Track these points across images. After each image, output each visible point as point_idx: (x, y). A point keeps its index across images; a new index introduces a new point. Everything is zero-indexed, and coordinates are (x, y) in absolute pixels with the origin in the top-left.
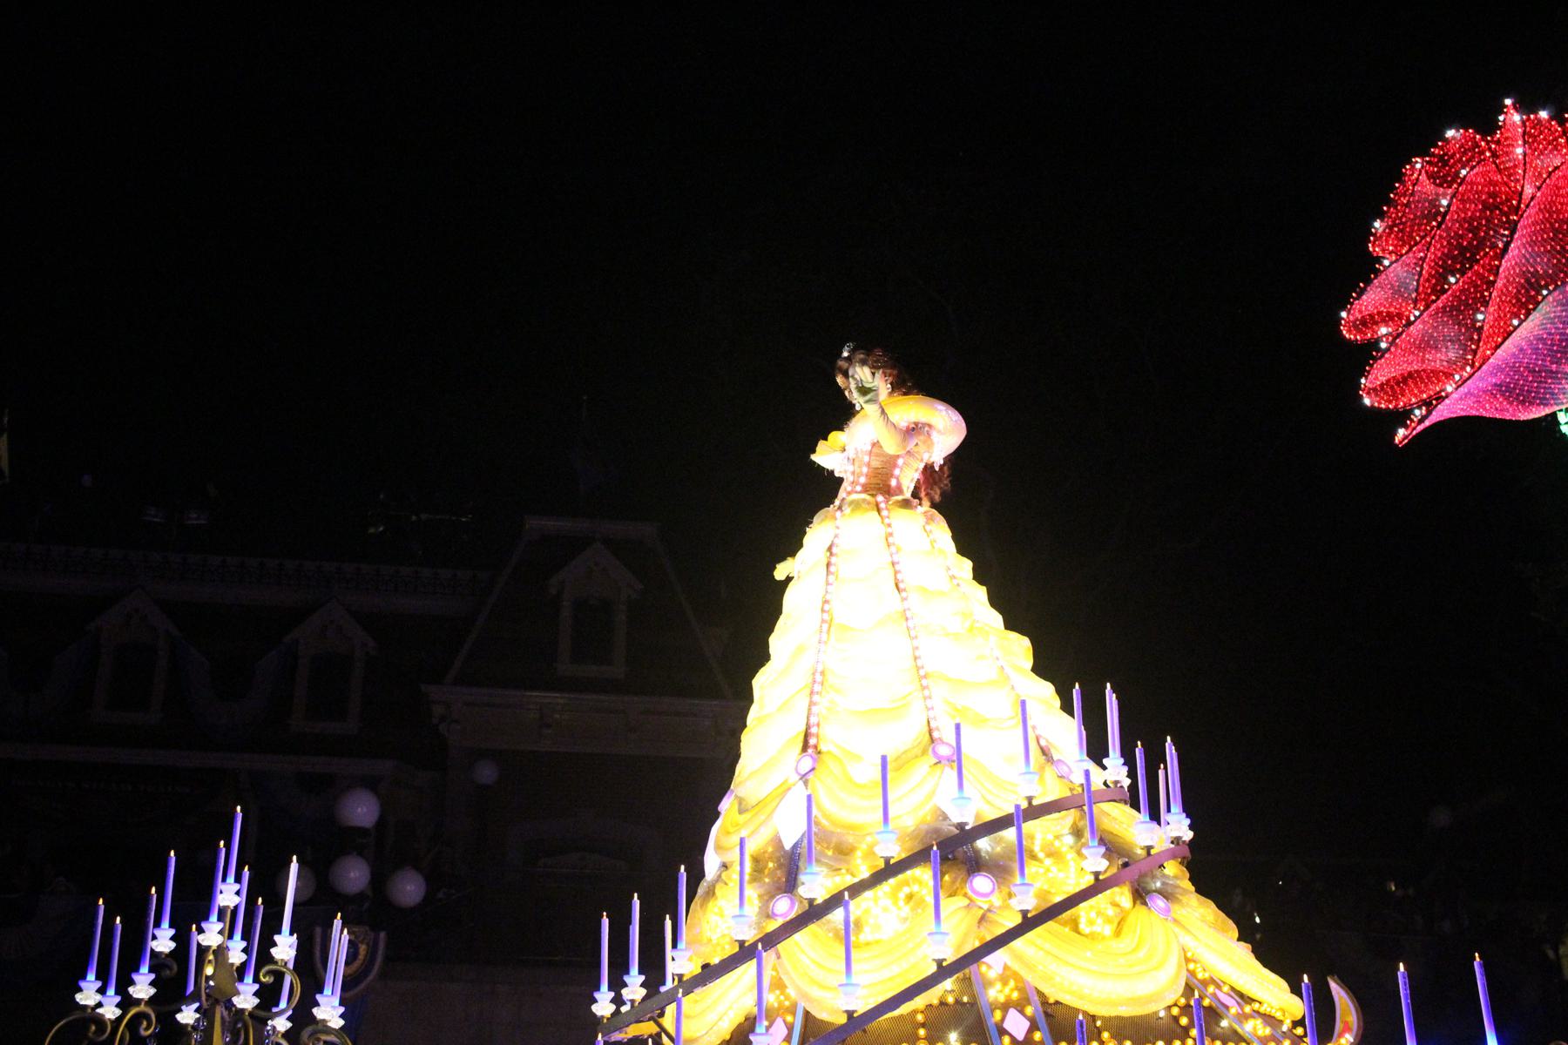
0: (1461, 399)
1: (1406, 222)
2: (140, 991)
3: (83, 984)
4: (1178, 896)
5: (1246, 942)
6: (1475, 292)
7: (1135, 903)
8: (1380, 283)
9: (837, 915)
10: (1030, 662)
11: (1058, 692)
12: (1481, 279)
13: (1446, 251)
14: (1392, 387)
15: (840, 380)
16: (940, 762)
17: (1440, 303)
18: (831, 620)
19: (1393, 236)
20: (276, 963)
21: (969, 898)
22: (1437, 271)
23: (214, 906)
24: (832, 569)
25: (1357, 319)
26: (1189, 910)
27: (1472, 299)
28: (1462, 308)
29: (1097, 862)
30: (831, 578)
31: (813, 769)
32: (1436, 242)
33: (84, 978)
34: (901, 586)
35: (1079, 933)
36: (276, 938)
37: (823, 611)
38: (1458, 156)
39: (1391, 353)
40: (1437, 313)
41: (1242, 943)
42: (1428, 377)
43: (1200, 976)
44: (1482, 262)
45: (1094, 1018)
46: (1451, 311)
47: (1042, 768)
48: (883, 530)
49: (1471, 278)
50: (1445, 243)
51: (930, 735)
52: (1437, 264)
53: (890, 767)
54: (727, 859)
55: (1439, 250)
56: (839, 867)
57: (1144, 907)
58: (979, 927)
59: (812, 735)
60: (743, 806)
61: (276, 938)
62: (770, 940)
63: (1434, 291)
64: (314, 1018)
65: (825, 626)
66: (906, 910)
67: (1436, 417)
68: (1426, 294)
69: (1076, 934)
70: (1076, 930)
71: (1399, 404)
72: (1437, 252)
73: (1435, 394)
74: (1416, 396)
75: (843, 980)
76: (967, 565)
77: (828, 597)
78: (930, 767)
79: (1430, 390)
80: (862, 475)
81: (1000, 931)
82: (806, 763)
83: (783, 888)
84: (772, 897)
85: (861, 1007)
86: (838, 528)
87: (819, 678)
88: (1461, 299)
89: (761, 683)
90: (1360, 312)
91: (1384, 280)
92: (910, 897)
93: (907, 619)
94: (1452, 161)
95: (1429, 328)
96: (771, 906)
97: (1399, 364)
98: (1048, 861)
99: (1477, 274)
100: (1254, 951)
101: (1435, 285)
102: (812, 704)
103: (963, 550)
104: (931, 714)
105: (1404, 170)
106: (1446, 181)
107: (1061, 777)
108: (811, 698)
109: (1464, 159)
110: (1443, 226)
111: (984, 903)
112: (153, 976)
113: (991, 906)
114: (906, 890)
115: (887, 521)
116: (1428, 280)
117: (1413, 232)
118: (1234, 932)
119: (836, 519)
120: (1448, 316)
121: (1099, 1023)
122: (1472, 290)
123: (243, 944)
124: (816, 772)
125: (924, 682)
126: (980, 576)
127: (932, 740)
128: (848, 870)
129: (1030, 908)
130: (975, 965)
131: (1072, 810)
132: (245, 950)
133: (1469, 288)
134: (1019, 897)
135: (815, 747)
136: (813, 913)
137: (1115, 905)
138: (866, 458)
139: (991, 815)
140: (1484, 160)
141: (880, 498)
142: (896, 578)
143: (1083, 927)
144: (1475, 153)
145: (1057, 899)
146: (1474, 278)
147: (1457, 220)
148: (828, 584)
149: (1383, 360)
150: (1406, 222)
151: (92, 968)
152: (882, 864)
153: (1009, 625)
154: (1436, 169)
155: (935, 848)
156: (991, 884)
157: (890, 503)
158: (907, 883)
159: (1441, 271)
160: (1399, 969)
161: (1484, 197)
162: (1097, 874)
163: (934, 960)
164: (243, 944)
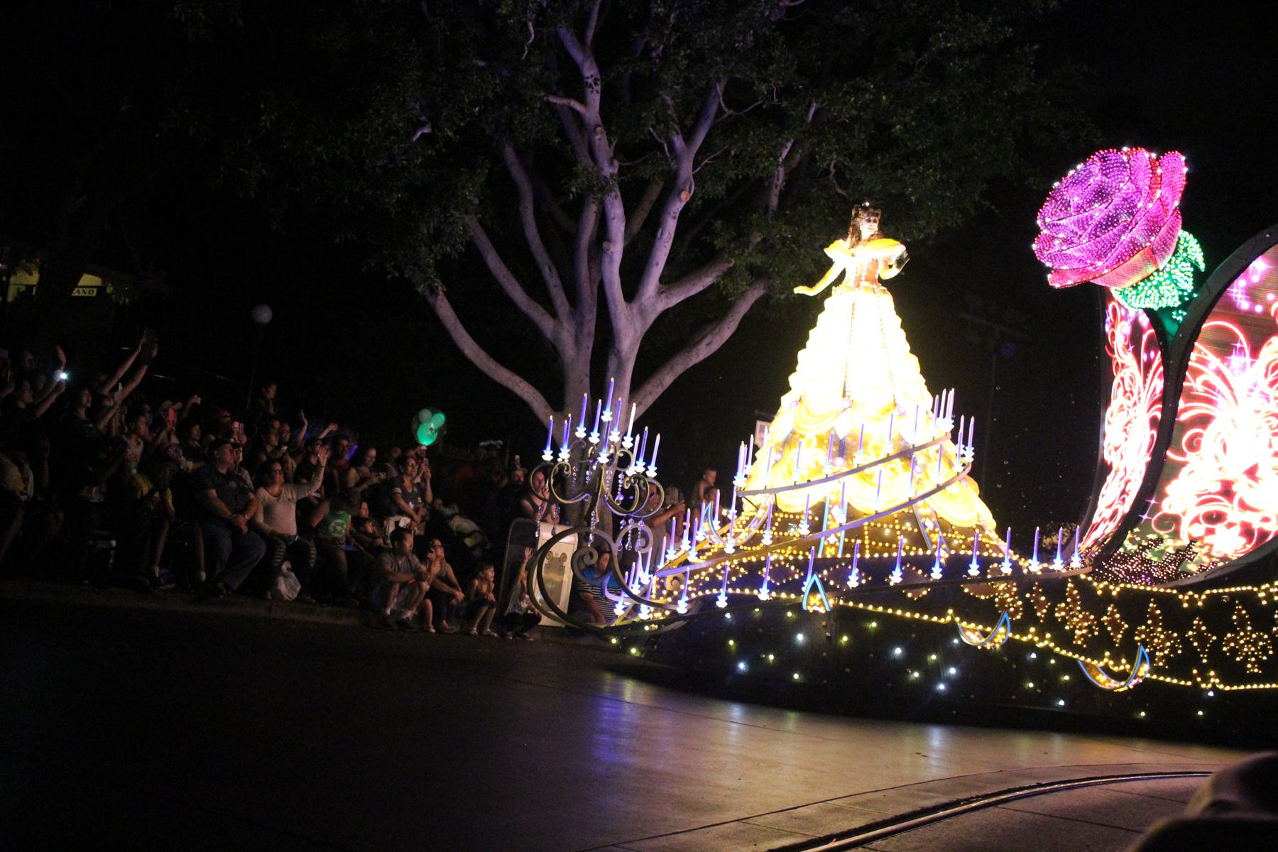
45: (951, 526)
81: (928, 490)
85: (880, 510)
121: (954, 527)
136: (859, 469)
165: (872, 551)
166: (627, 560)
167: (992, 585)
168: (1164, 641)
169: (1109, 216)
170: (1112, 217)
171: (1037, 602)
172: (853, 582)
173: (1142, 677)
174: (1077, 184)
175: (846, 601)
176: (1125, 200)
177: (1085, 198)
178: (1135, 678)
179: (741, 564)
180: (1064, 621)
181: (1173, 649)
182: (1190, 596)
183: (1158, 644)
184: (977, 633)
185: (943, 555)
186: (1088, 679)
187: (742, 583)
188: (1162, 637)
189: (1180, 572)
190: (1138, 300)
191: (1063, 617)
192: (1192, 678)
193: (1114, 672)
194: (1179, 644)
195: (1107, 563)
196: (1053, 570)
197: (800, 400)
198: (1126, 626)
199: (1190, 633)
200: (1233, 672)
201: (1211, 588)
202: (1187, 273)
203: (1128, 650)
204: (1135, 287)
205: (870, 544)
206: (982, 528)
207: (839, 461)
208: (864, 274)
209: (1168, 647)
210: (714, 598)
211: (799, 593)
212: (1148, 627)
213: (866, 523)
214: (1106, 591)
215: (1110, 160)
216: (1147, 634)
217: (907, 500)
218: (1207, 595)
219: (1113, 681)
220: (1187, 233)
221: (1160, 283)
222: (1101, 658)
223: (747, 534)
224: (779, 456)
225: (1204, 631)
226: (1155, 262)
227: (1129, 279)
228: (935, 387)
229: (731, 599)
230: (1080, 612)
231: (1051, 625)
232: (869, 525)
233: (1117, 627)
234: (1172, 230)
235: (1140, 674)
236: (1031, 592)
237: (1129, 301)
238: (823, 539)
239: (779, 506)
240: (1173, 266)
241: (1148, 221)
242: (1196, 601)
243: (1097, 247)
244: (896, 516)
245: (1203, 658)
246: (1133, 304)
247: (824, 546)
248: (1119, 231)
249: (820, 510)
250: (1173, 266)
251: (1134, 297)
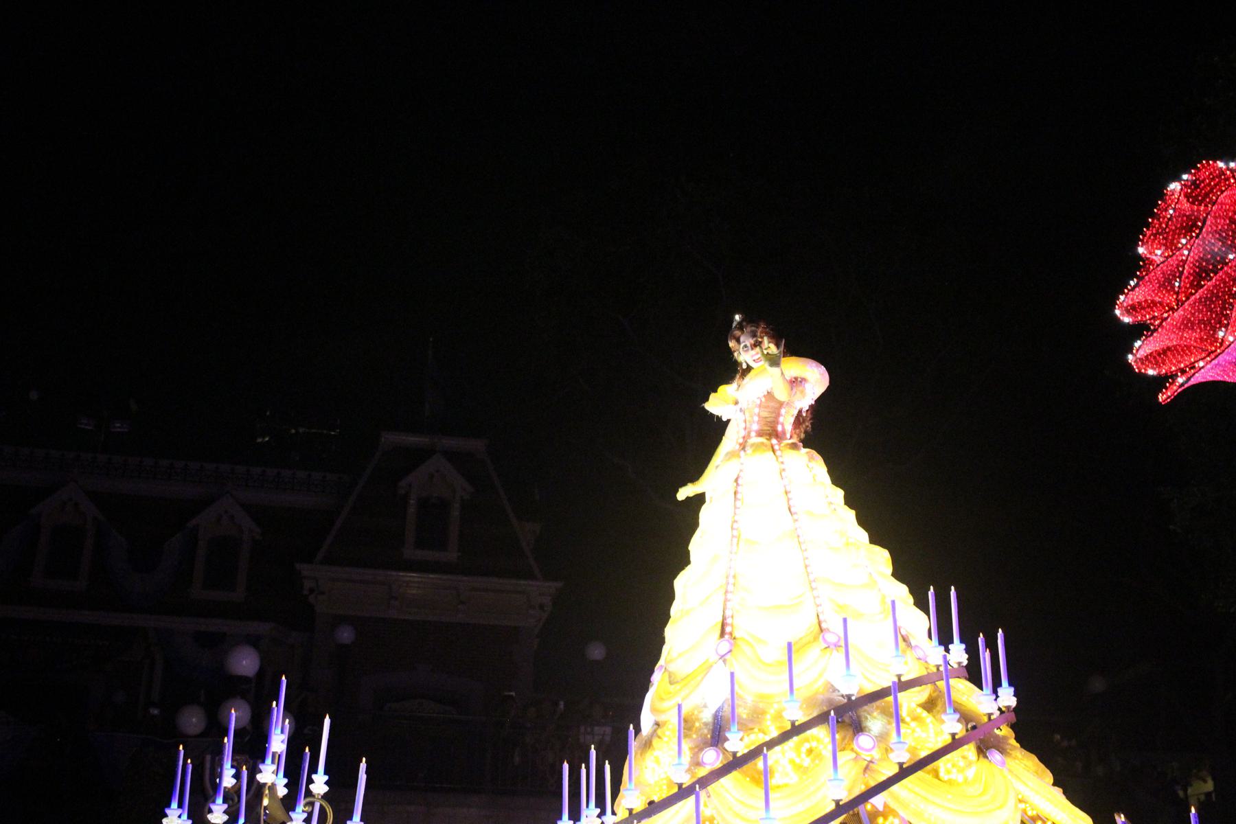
0: (1212, 368)
1: (1169, 232)
2: (216, 818)
3: (168, 811)
4: (1008, 751)
5: (1059, 787)
6: (1225, 287)
7: (979, 757)
8: (1149, 278)
9: (759, 762)
10: (890, 569)
11: (912, 592)
12: (1228, 277)
13: (1202, 256)
14: (1155, 358)
15: (732, 344)
16: (829, 647)
17: (1197, 296)
18: (740, 535)
19: (1156, 242)
20: (314, 796)
21: (856, 753)
22: (1195, 271)
23: (269, 753)
24: (739, 496)
25: (1129, 305)
26: (1017, 761)
27: (1222, 292)
28: (1214, 299)
29: (953, 726)
31: (730, 651)
32: (1195, 248)
33: (169, 806)
34: (792, 510)
35: (939, 779)
37: (732, 529)
38: (1207, 181)
39: (1158, 333)
40: (1195, 303)
41: (1056, 788)
42: (1183, 350)
43: (1031, 813)
44: (1230, 264)
46: (1205, 302)
47: (904, 651)
49: (1221, 277)
50: (1201, 249)
51: (820, 626)
52: (1194, 265)
53: (794, 648)
54: (661, 719)
55: (1197, 254)
56: (752, 727)
57: (986, 760)
58: (864, 775)
59: (727, 624)
60: (672, 679)
62: (704, 782)
63: (1192, 286)
65: (735, 540)
66: (807, 761)
67: (1193, 381)
68: (1186, 287)
69: (937, 781)
70: (937, 776)
71: (1162, 371)
72: (1195, 256)
73: (1191, 364)
74: (1174, 365)
75: (763, 813)
76: (839, 493)
77: (737, 518)
78: (821, 650)
79: (1185, 361)
80: (754, 422)
81: (882, 778)
82: (724, 646)
83: (710, 742)
84: (701, 749)
86: (742, 464)
87: (731, 580)
88: (1213, 293)
89: (682, 583)
90: (1132, 299)
91: (1153, 276)
92: (810, 751)
94: (1203, 185)
95: (1188, 314)
96: (701, 756)
97: (1162, 341)
98: (913, 724)
99: (1227, 274)
100: (1065, 793)
101: (1193, 281)
102: (726, 600)
103: (836, 481)
104: (820, 609)
105: (1165, 191)
106: (1197, 200)
107: (919, 659)
108: (726, 596)
109: (1212, 183)
110: (1200, 237)
111: (867, 756)
112: (225, 806)
113: (873, 758)
114: (807, 746)
115: (780, 459)
116: (1188, 277)
117: (1174, 240)
118: (1049, 778)
119: (740, 457)
120: (1203, 305)
122: (1222, 285)
123: (233, 771)
124: (733, 653)
125: (814, 585)
126: (849, 502)
127: (821, 630)
128: (759, 730)
129: (905, 761)
130: (862, 805)
131: (929, 685)
132: (235, 776)
133: (1220, 284)
134: (896, 752)
135: (731, 634)
136: (735, 763)
137: (964, 757)
138: (757, 410)
139: (870, 688)
140: (1229, 185)
141: (774, 441)
142: (788, 504)
143: (942, 774)
144: (1222, 179)
145: (923, 754)
146: (1224, 277)
147: (1210, 232)
148: (736, 508)
149: (1152, 338)
150: (1169, 232)
151: (175, 797)
152: (789, 727)
153: (874, 540)
154: (1189, 191)
155: (832, 713)
156: (872, 742)
157: (782, 445)
158: (807, 740)
159: (1197, 270)
160: (1190, 811)
161: (1230, 214)
162: (953, 735)
163: (833, 800)
164: (233, 771)
208: (755, 427)
217: (832, 806)
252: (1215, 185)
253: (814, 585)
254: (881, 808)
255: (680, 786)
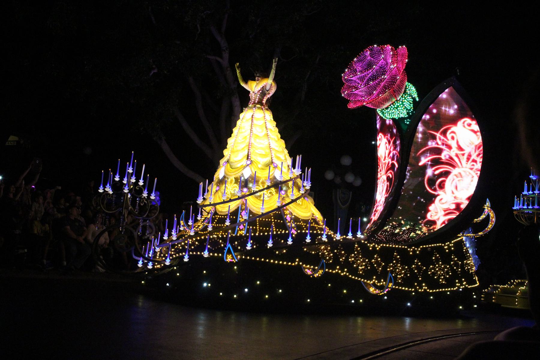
10: (285, 146)
24: (253, 121)
30: (253, 123)
31: (250, 164)
36: (140, 180)
45: (299, 219)
48: (263, 115)
61: (140, 180)
64: (150, 198)
66: (270, 195)
75: (262, 207)
81: (287, 202)
82: (249, 162)
85: (265, 211)
93: (268, 136)
99: (376, 82)
121: (300, 220)
125: (271, 150)
158: (270, 190)
165: (260, 232)
166: (144, 241)
167: (318, 246)
168: (401, 270)
169: (374, 75)
170: (375, 76)
171: (340, 254)
172: (249, 247)
173: (390, 288)
174: (360, 61)
175: (246, 256)
176: (381, 68)
177: (363, 67)
178: (387, 288)
179: (197, 240)
180: (353, 262)
181: (405, 274)
182: (413, 249)
183: (399, 272)
184: (310, 270)
185: (294, 232)
186: (365, 289)
187: (196, 250)
188: (400, 268)
189: (410, 238)
190: (388, 114)
191: (352, 261)
192: (415, 287)
193: (378, 285)
194: (408, 271)
195: (377, 235)
196: (348, 239)
197: (228, 161)
198: (383, 264)
199: (413, 266)
200: (433, 283)
201: (423, 245)
202: (410, 102)
203: (383, 275)
204: (387, 108)
205: (259, 229)
206: (315, 221)
207: (245, 190)
209: (403, 273)
210: (183, 257)
211: (223, 254)
212: (394, 264)
213: (258, 219)
214: (374, 247)
215: (374, 50)
216: (393, 268)
218: (421, 248)
219: (377, 290)
220: (409, 84)
221: (398, 107)
222: (371, 280)
223: (202, 226)
224: (218, 188)
225: (420, 265)
226: (396, 97)
227: (384, 104)
228: (292, 154)
229: (190, 257)
230: (361, 258)
231: (347, 265)
232: (259, 220)
233: (379, 265)
234: (402, 82)
235: (389, 286)
236: (337, 249)
237: (385, 115)
238: (237, 226)
239: (217, 212)
240: (403, 99)
241: (391, 77)
242: (416, 251)
243: (368, 89)
244: (272, 215)
245: (420, 277)
246: (387, 117)
247: (238, 230)
248: (378, 82)
249: (236, 213)
250: (403, 99)
251: (387, 113)
252: (377, 53)
253: (271, 150)
254: (285, 208)
255: (239, 196)
